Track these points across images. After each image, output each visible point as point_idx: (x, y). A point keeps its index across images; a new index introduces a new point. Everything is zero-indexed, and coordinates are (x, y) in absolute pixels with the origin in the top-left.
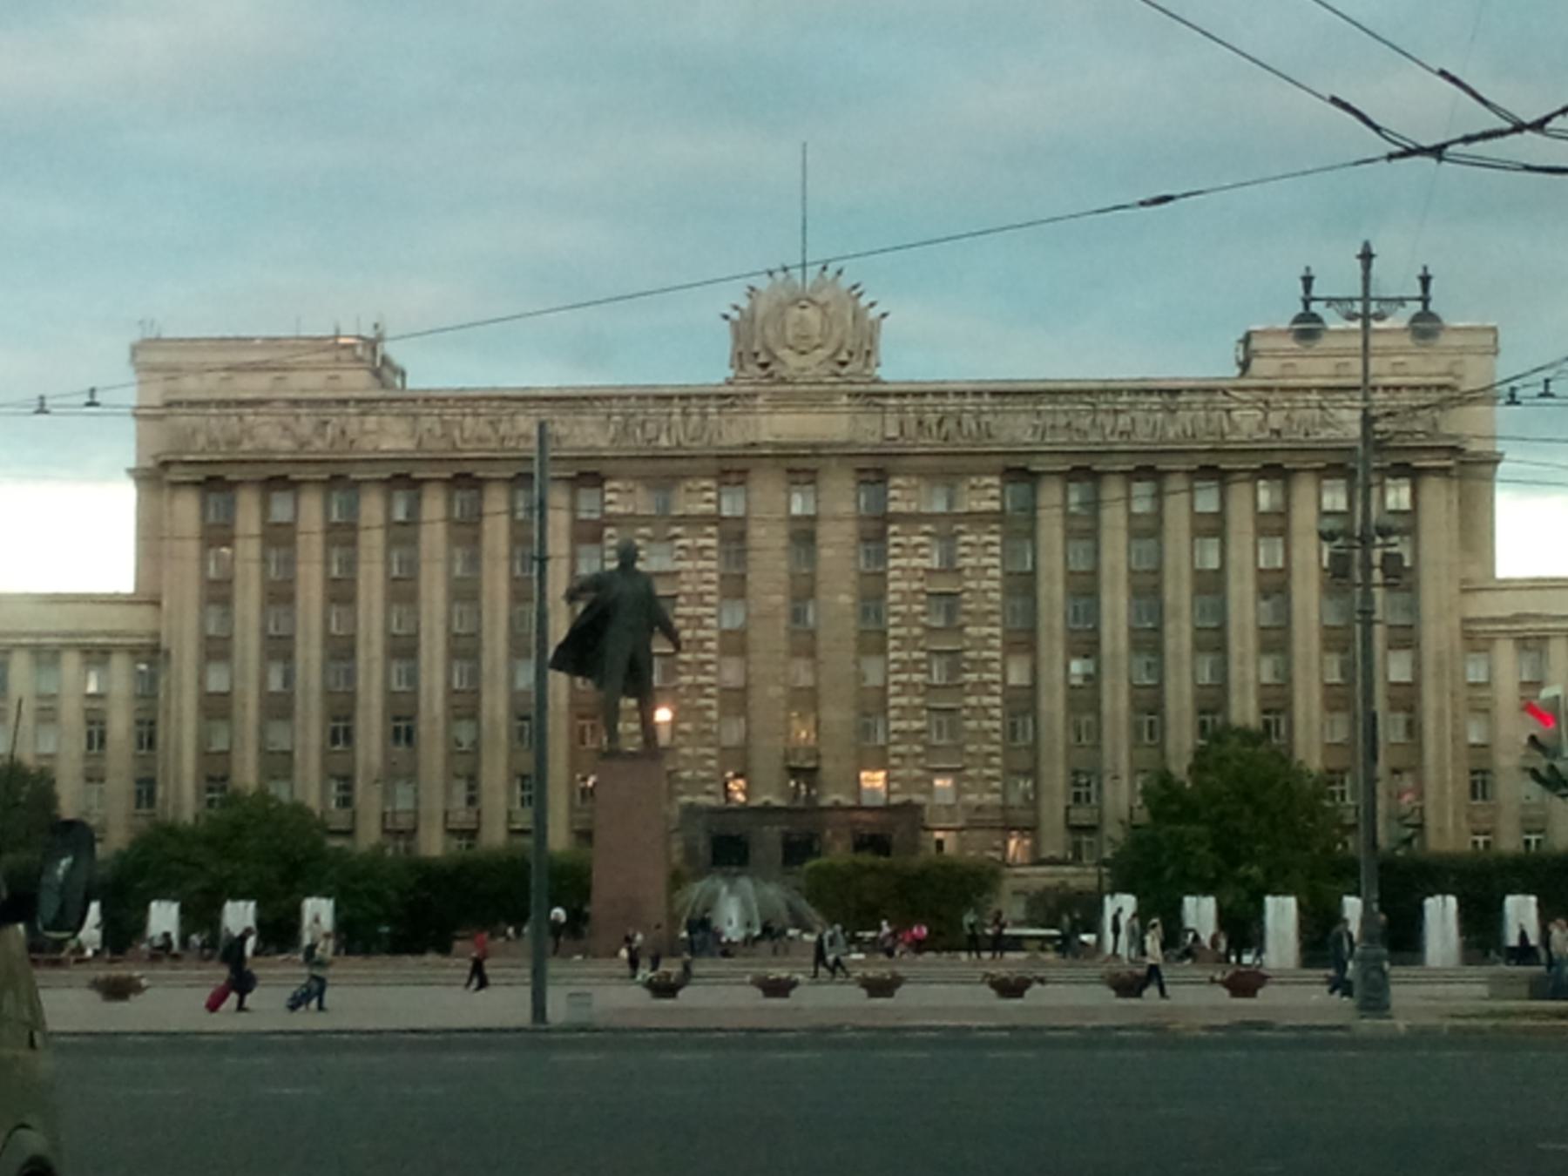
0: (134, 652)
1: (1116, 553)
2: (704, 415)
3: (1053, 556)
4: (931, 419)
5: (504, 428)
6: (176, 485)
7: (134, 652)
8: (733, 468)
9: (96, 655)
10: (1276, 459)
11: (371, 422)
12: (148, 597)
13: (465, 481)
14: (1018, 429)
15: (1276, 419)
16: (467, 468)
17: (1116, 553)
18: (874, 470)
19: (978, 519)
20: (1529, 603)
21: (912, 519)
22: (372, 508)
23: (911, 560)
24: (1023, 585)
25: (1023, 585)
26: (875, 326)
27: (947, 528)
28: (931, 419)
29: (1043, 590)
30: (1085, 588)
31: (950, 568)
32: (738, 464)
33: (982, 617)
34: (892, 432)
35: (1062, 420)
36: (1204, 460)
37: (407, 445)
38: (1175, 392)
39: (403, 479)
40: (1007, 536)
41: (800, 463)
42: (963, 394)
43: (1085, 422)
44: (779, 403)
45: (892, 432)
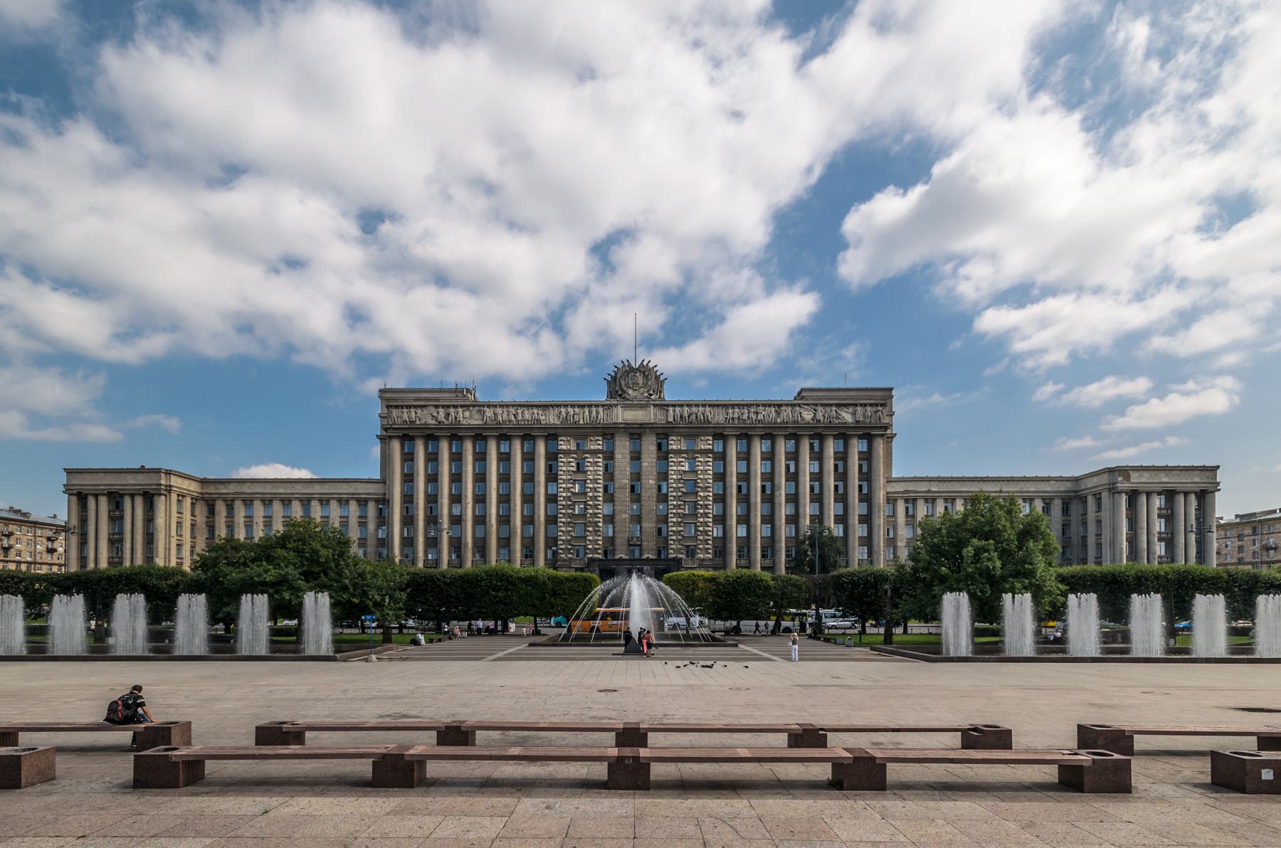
0: (377, 501)
1: (758, 467)
2: (597, 413)
3: (734, 467)
4: (686, 414)
5: (520, 417)
6: (391, 438)
7: (377, 501)
8: (609, 432)
9: (343, 502)
10: (819, 431)
11: (467, 414)
12: (383, 481)
13: (504, 436)
14: (718, 417)
15: (820, 415)
16: (505, 431)
17: (758, 467)
18: (663, 433)
19: (705, 452)
20: (911, 486)
21: (678, 452)
22: (468, 446)
23: (679, 466)
24: (721, 477)
25: (721, 477)
26: (663, 382)
27: (691, 454)
28: (686, 414)
29: (728, 479)
30: (745, 477)
31: (693, 471)
32: (611, 431)
33: (705, 489)
34: (671, 419)
35: (736, 415)
36: (791, 431)
37: (480, 422)
38: (780, 406)
39: (479, 436)
40: (714, 459)
41: (635, 432)
42: (698, 406)
43: (745, 417)
44: (626, 407)
45: (671, 419)
